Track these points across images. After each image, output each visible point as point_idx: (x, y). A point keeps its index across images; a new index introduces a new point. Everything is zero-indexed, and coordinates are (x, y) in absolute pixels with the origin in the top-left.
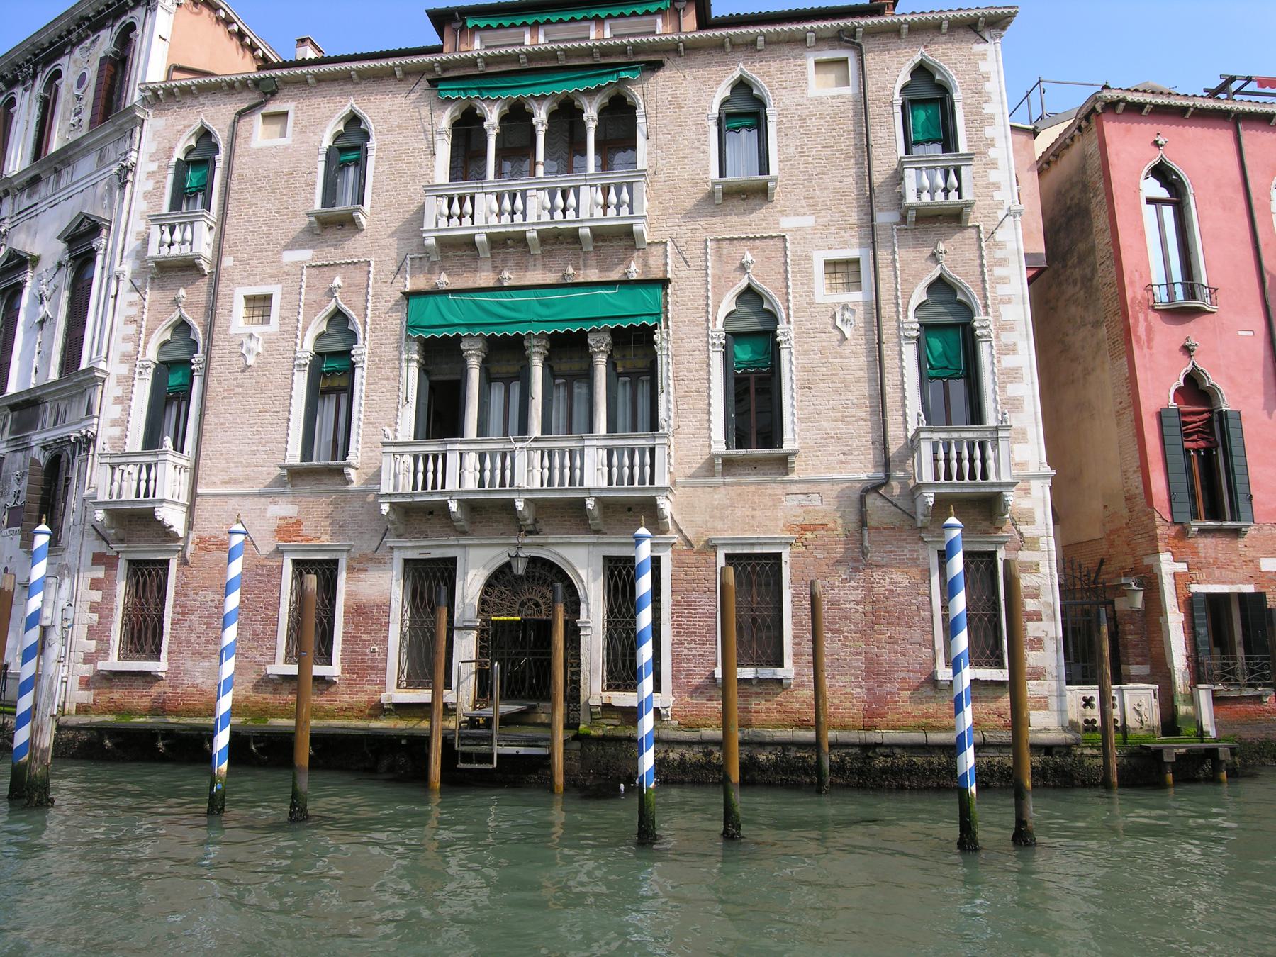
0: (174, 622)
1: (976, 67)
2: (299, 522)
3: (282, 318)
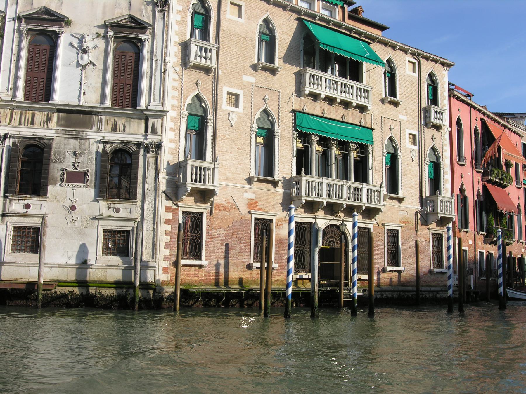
0: (207, 242)
1: (443, 79)
2: (257, 202)
3: (245, 108)
